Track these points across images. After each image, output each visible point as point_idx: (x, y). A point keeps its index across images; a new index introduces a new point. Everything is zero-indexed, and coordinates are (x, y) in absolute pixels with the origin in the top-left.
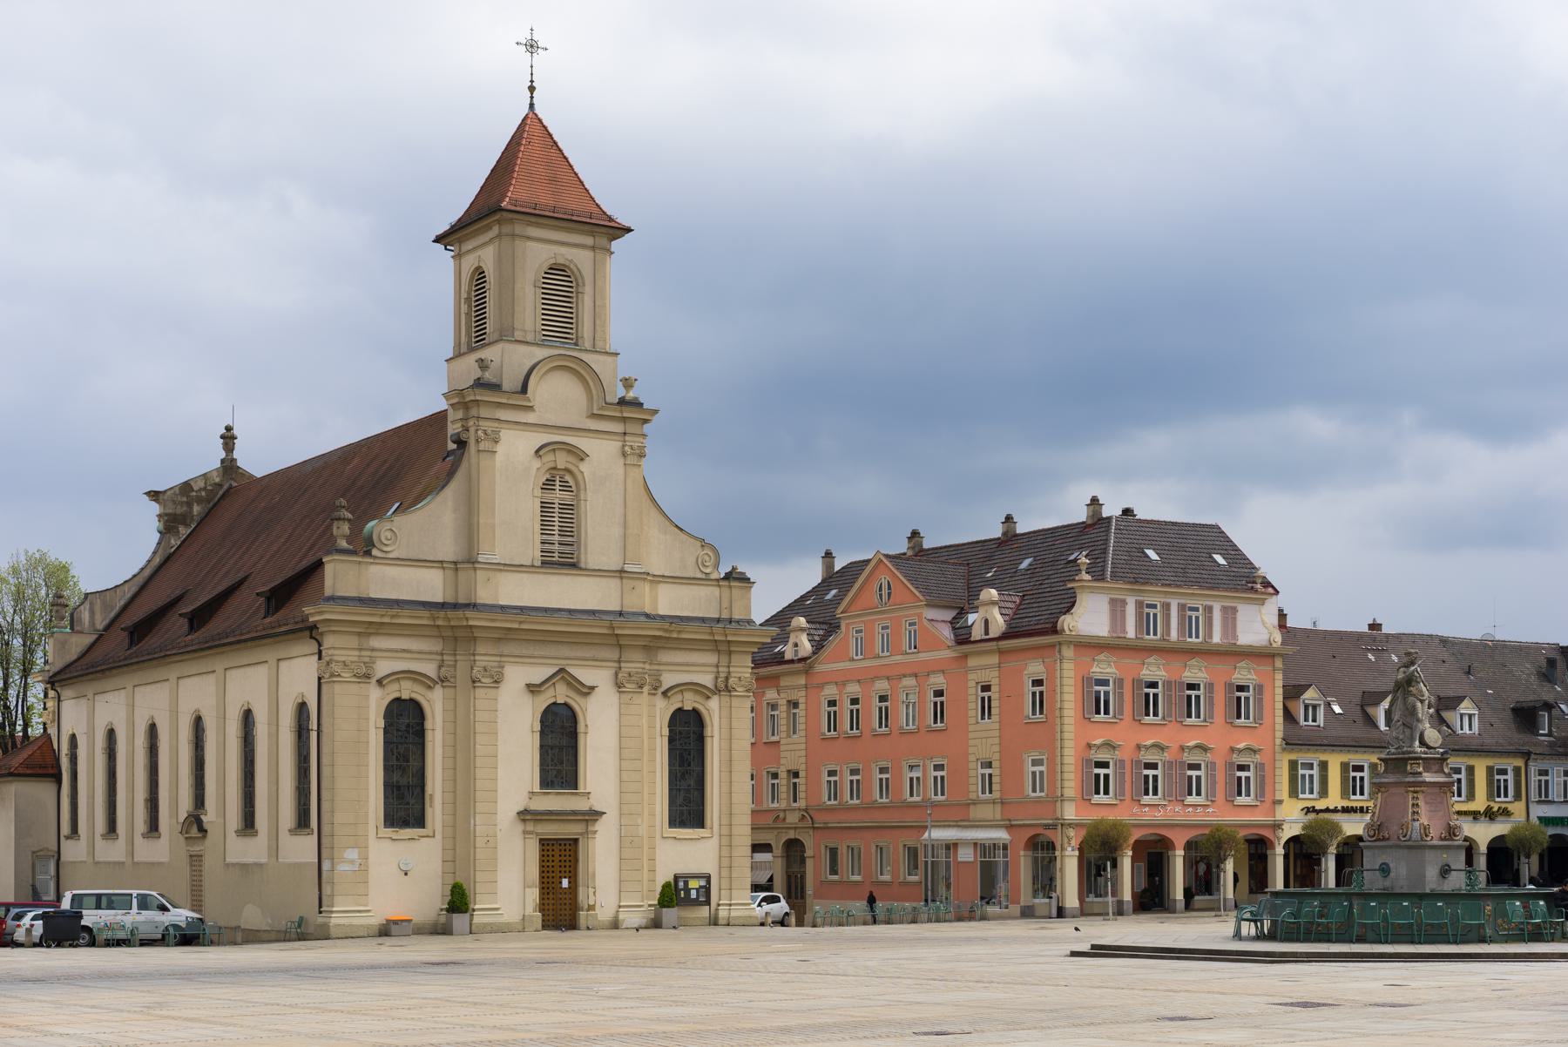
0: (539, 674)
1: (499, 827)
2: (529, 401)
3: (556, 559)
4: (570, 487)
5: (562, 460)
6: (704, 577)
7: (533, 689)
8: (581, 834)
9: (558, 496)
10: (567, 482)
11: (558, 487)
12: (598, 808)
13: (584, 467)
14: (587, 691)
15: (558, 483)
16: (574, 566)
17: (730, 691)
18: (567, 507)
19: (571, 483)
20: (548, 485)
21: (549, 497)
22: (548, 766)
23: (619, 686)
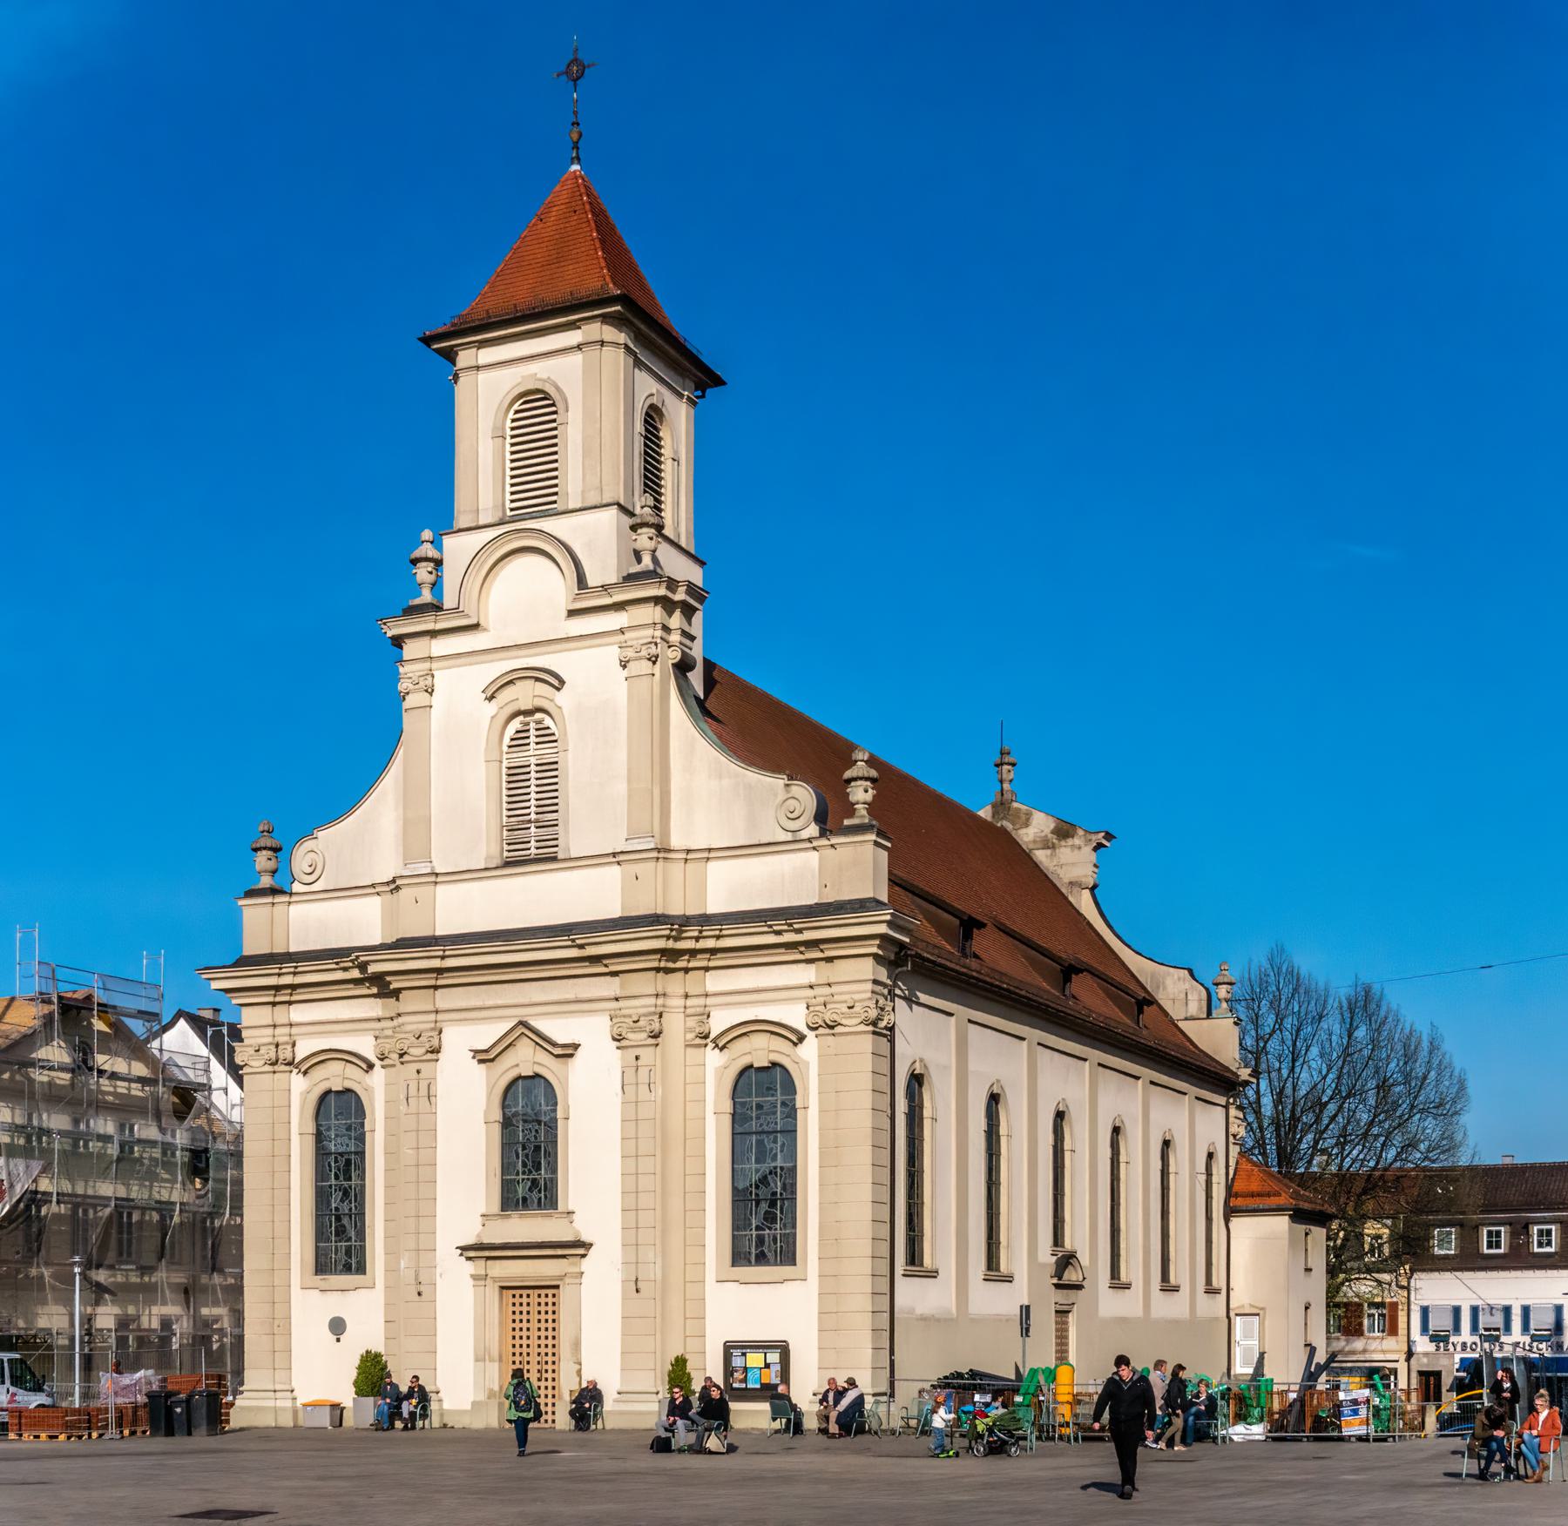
0: (487, 1034)
1: (438, 1271)
2: (467, 616)
3: (533, 851)
4: (553, 734)
5: (525, 694)
6: (789, 837)
7: (484, 1057)
8: (561, 1278)
9: (533, 754)
10: (548, 728)
11: (533, 739)
12: (585, 1238)
13: (561, 698)
14: (568, 1052)
15: (533, 732)
16: (554, 859)
17: (832, 1027)
18: (549, 767)
19: (554, 729)
20: (520, 740)
21: (519, 758)
22: (518, 1174)
23: (618, 1039)
